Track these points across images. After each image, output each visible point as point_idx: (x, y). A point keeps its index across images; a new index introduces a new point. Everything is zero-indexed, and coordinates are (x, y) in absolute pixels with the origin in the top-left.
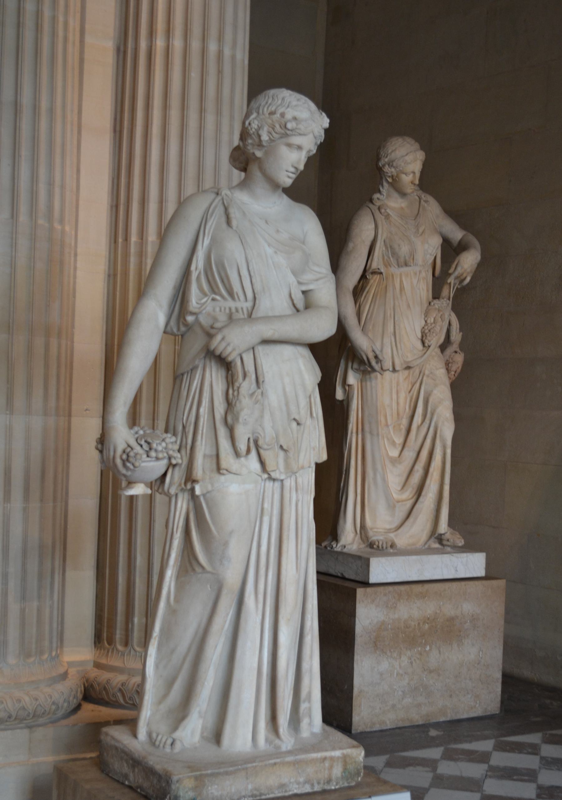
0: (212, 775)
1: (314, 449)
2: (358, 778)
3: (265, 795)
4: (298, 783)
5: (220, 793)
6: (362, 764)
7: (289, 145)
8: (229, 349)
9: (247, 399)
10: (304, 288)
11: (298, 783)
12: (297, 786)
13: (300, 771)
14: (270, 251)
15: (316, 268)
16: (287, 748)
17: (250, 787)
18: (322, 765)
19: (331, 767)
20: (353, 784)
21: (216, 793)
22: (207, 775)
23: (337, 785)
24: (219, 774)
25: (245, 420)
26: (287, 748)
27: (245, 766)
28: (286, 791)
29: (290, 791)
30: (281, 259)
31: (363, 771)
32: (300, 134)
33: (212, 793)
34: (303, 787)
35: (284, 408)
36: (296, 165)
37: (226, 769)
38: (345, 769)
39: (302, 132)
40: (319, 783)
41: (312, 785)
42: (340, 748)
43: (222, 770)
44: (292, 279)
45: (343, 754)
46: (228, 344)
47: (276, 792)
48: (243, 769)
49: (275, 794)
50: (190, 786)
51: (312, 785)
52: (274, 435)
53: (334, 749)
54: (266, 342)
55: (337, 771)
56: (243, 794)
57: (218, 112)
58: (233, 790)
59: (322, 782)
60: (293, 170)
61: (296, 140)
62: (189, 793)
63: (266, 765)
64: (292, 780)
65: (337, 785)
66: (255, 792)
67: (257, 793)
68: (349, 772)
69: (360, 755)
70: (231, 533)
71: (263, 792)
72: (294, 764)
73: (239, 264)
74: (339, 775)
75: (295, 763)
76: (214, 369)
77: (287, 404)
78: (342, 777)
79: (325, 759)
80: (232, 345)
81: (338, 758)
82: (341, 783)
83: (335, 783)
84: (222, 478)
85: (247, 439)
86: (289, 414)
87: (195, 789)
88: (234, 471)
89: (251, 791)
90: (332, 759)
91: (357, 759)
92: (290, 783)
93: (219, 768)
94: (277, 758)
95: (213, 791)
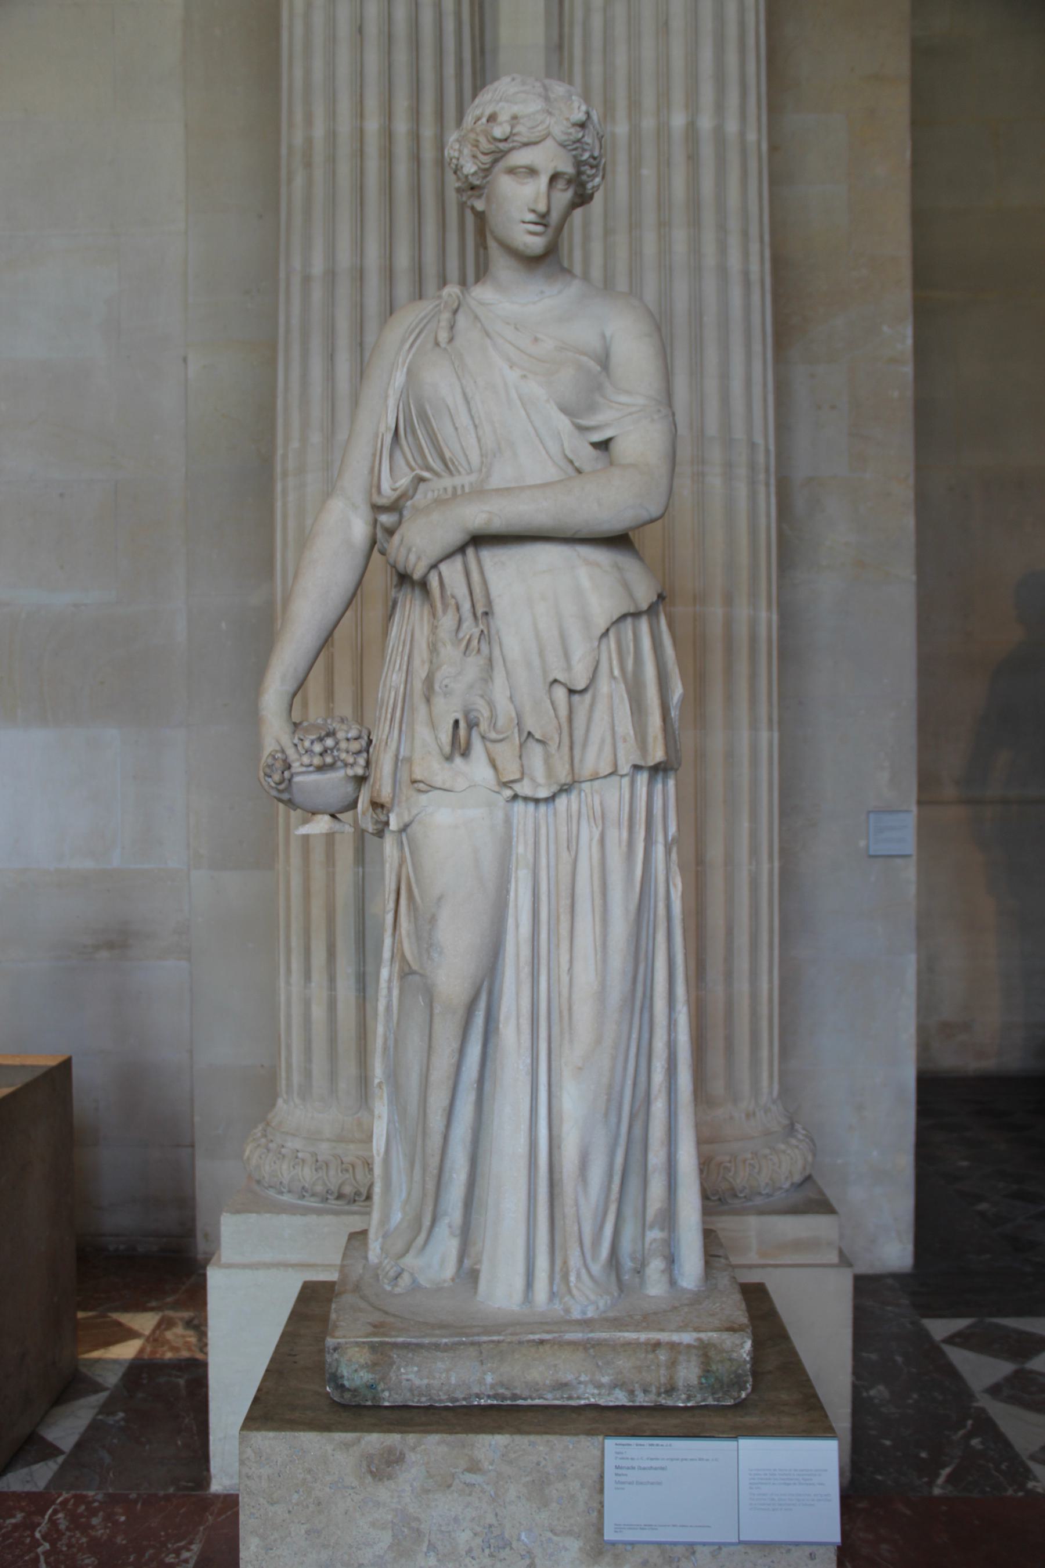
0: (406, 1346)
1: (625, 741)
2: (739, 1392)
3: (525, 1399)
4: (599, 1386)
5: (426, 1381)
6: (748, 1366)
7: (512, 171)
8: (412, 558)
9: (449, 647)
10: (597, 437)
11: (599, 1386)
12: (596, 1391)
13: (600, 1363)
14: (513, 376)
15: (623, 399)
16: (584, 1313)
17: (489, 1379)
18: (651, 1356)
19: (673, 1364)
20: (730, 1402)
21: (417, 1382)
22: (395, 1345)
23: (689, 1399)
24: (420, 1346)
25: (446, 686)
26: (584, 1313)
27: (476, 1339)
28: (570, 1398)
29: (579, 1398)
30: (535, 388)
31: (750, 1379)
32: (526, 145)
33: (408, 1380)
34: (609, 1394)
35: (536, 662)
36: (533, 207)
37: (434, 1340)
38: (706, 1372)
39: (525, 140)
40: (646, 1391)
41: (632, 1393)
42: (697, 1330)
43: (426, 1341)
44: (564, 423)
45: (699, 1340)
46: (409, 550)
47: (549, 1396)
48: (473, 1344)
49: (546, 1399)
50: (362, 1361)
51: (632, 1393)
52: (514, 715)
53: (680, 1329)
54: (479, 540)
55: (688, 1373)
56: (476, 1390)
57: (695, 222)
58: (453, 1380)
59: (654, 1389)
60: (531, 217)
61: (521, 158)
62: (362, 1374)
63: (520, 1343)
64: (583, 1378)
65: (689, 1399)
66: (501, 1391)
67: (508, 1393)
68: (717, 1379)
69: (742, 1345)
70: (440, 898)
71: (518, 1392)
72: (586, 1349)
73: (451, 406)
74: (694, 1381)
75: (585, 1346)
76: (418, 602)
77: (541, 654)
78: (701, 1387)
79: (657, 1345)
80: (414, 549)
81: (689, 1346)
82: (699, 1397)
83: (683, 1396)
84: (423, 798)
85: (451, 722)
86: (545, 672)
87: (372, 1367)
88: (439, 784)
89: (492, 1386)
90: (673, 1347)
91: (735, 1355)
92: (580, 1383)
93: (424, 1337)
94: (548, 1332)
95: (411, 1376)
